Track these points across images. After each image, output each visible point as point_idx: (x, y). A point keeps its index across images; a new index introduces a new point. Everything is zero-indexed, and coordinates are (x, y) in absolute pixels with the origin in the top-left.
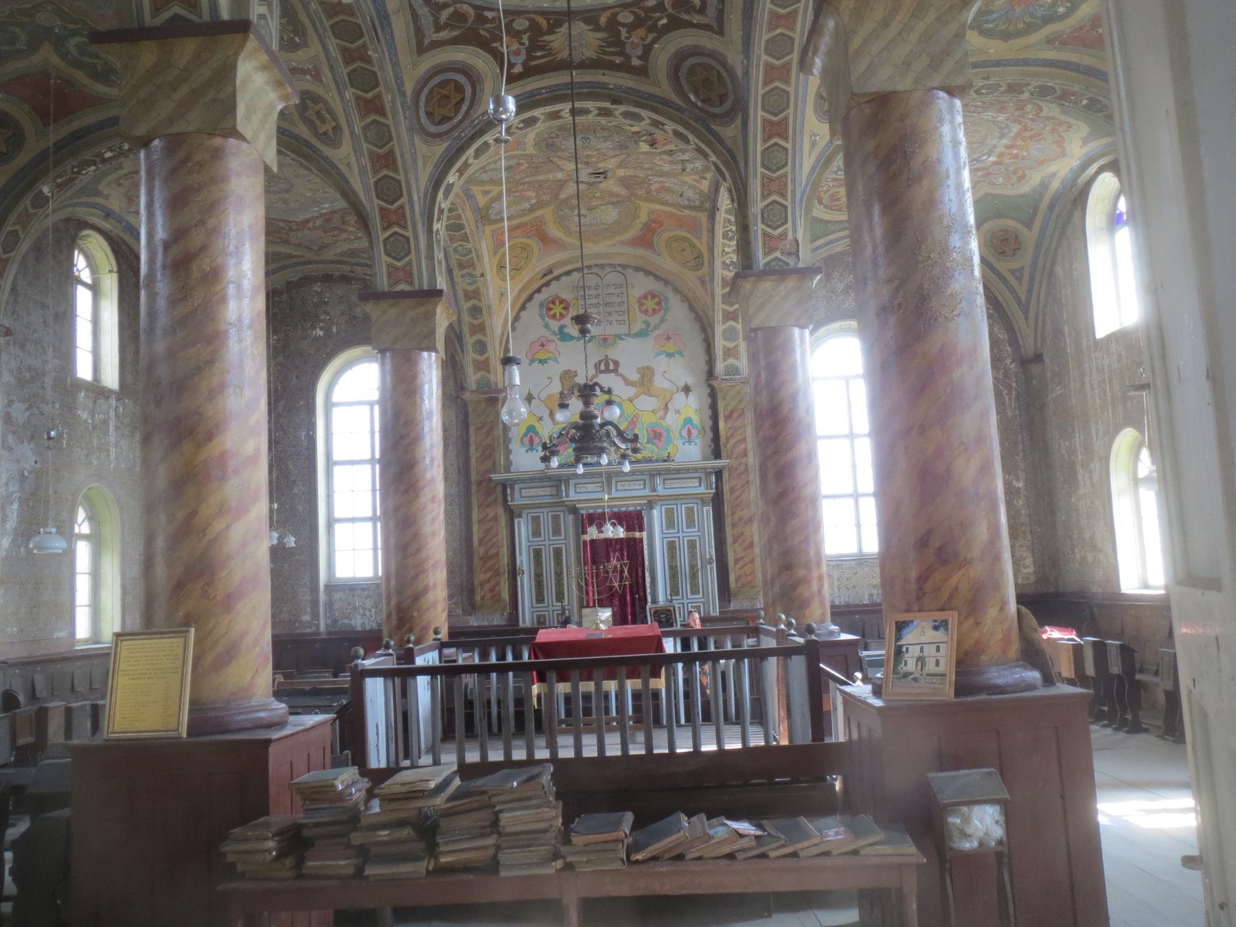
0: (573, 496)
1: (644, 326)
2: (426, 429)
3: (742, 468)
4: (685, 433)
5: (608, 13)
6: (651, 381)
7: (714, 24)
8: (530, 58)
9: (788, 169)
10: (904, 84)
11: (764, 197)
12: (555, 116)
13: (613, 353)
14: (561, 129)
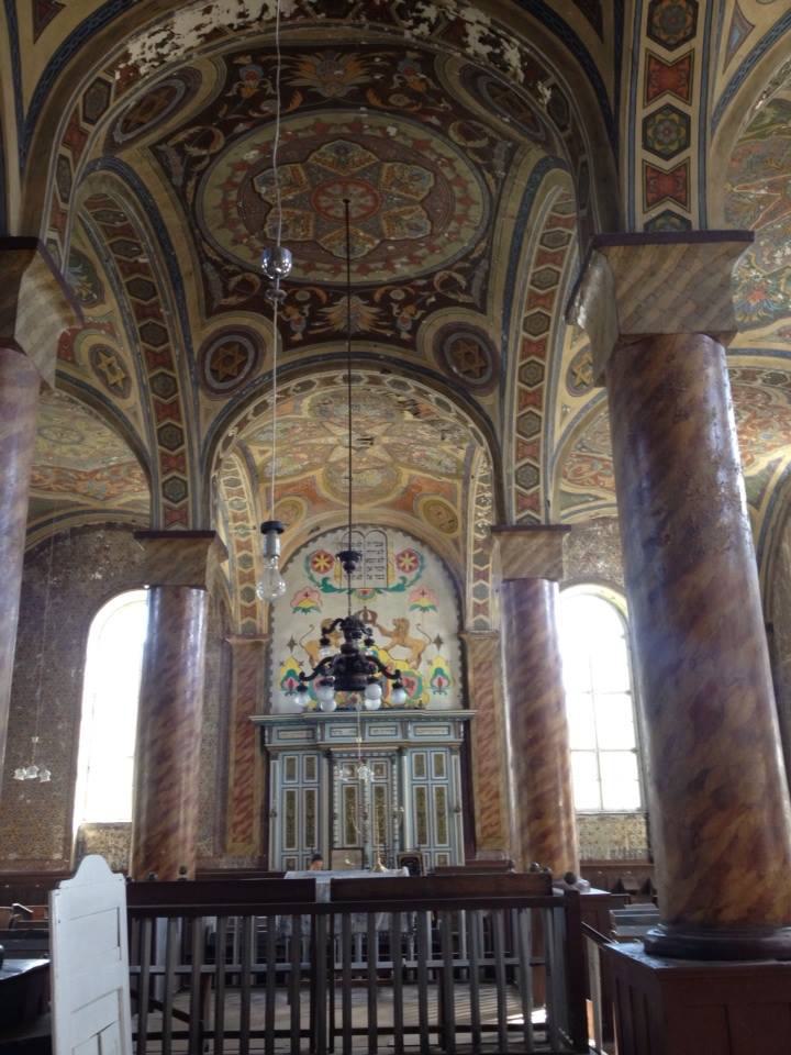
0: (328, 740)
1: (401, 582)
2: (189, 664)
3: (488, 719)
4: (435, 683)
5: (383, 290)
6: (405, 633)
7: (478, 304)
8: (309, 327)
9: (541, 435)
10: (671, 328)
11: (518, 460)
12: (329, 382)
13: (371, 605)
14: (335, 395)
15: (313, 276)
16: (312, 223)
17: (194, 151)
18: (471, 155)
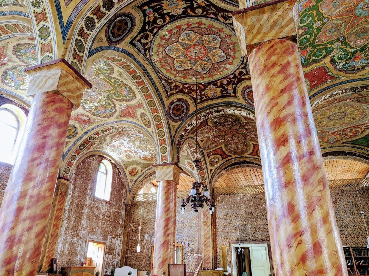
5: (167, 22)
15: (197, 20)
16: (204, 42)
17: (244, 71)
18: (172, 81)
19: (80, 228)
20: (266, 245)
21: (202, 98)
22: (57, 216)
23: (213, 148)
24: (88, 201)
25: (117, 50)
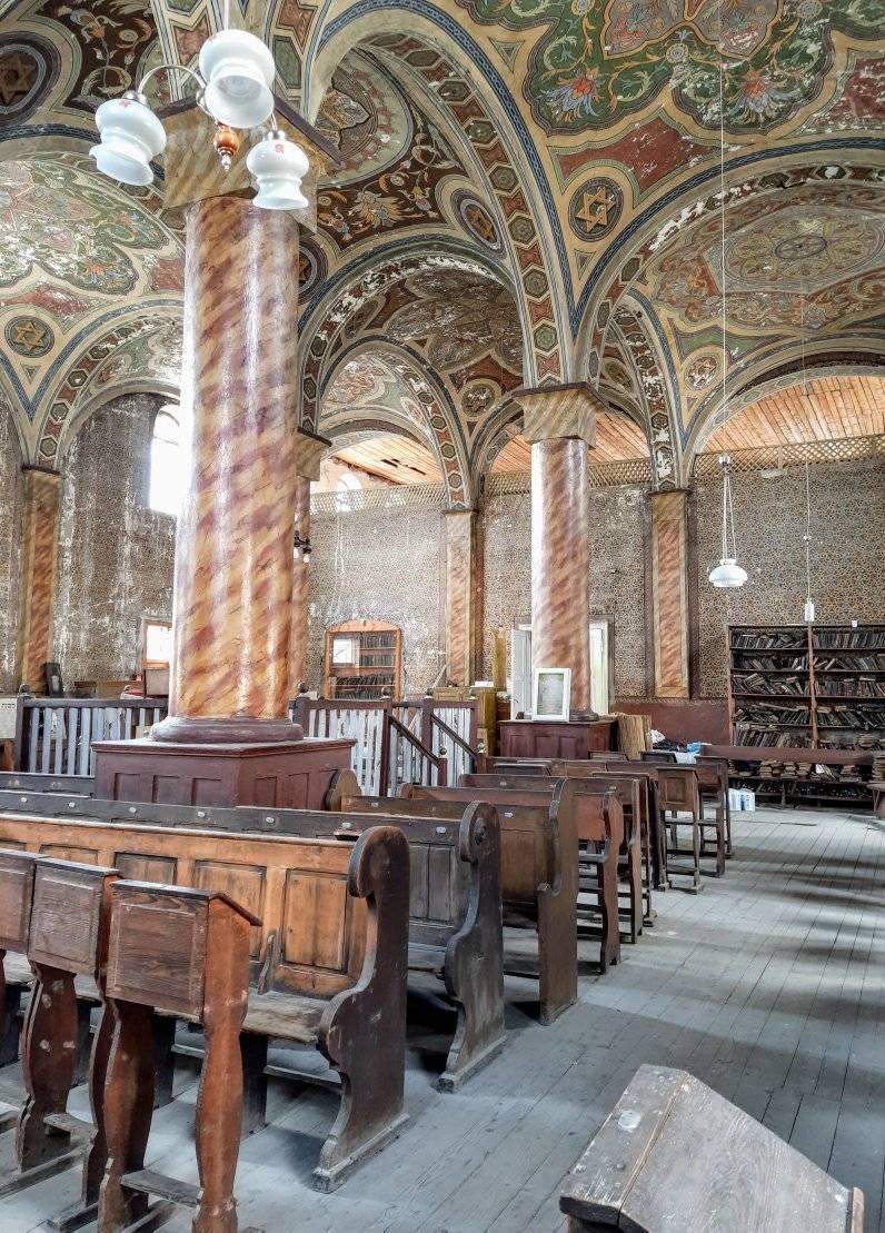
7: (79, 99)
19: (116, 591)
20: (605, 626)
21: (352, 229)
22: (40, 566)
23: (463, 360)
24: (129, 523)
25: (32, 133)
